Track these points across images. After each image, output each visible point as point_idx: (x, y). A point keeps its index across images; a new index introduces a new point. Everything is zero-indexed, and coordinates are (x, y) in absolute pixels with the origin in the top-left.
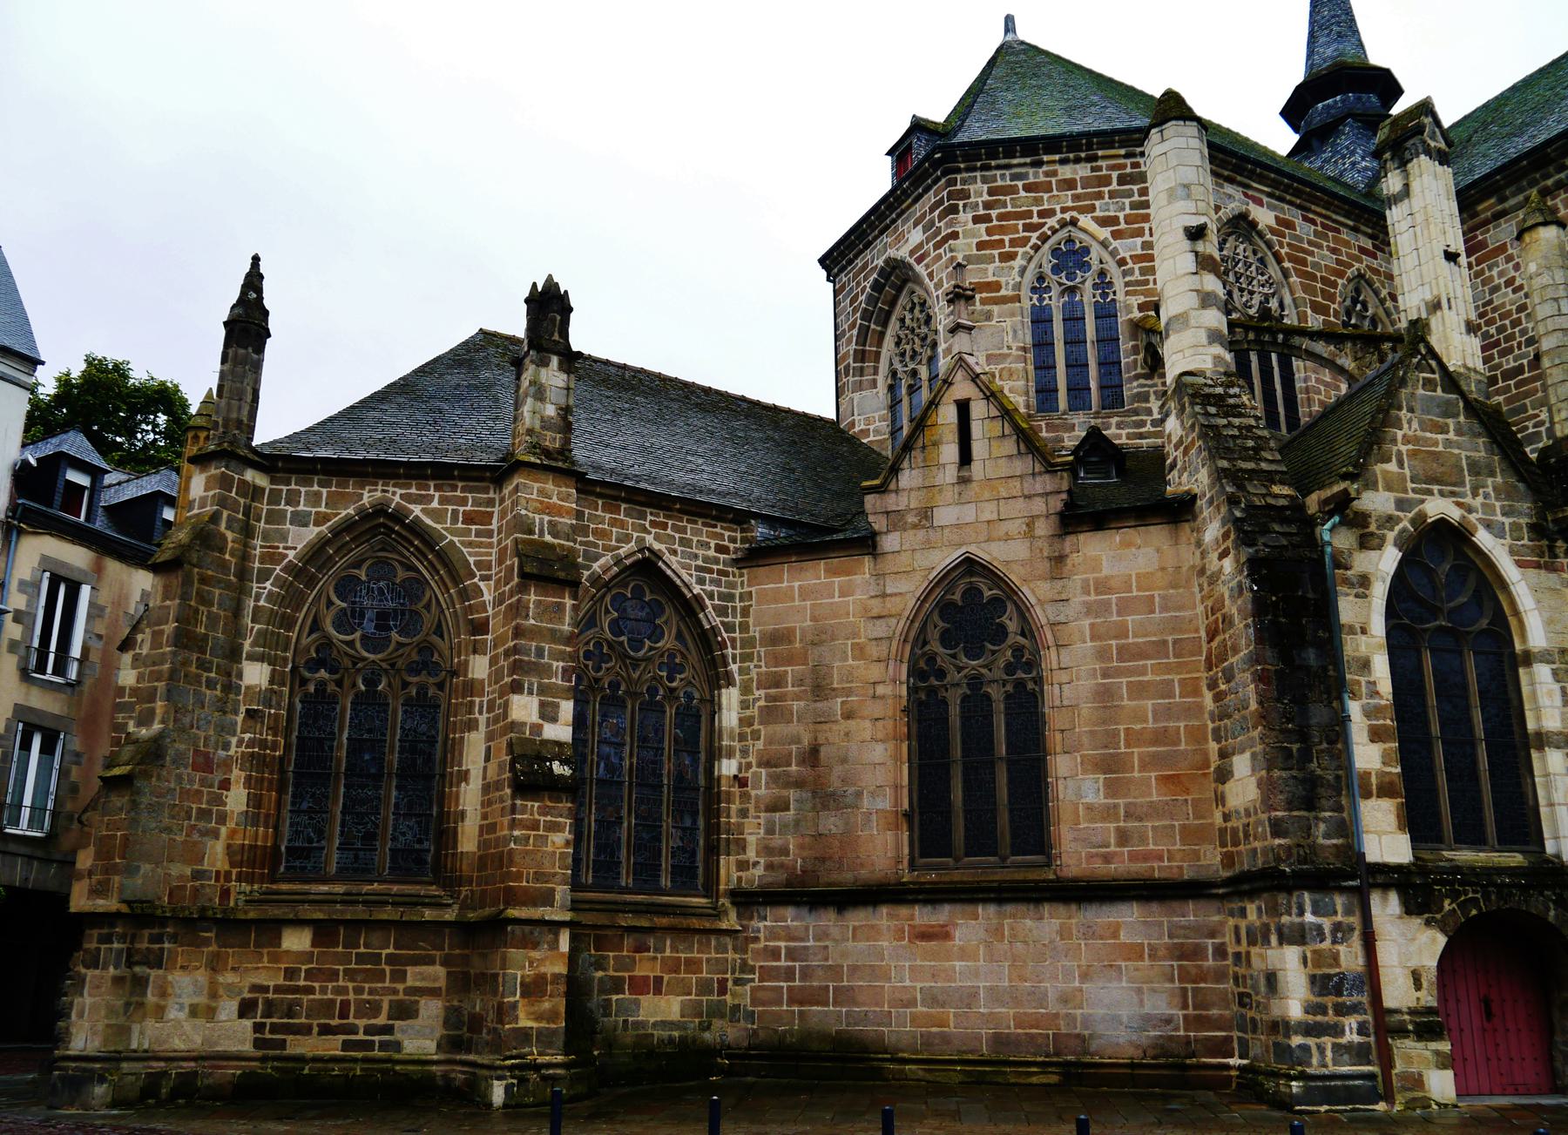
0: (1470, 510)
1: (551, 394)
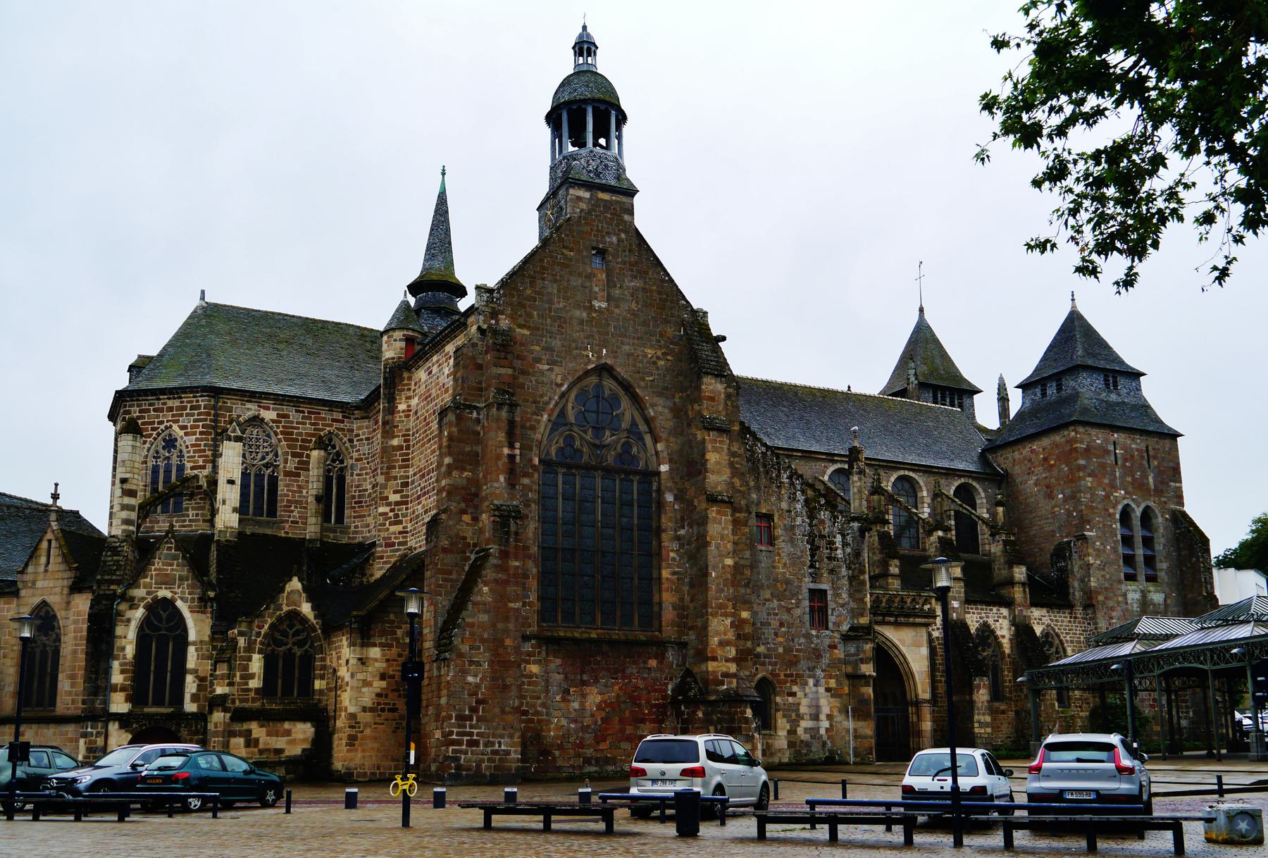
0: (175, 593)
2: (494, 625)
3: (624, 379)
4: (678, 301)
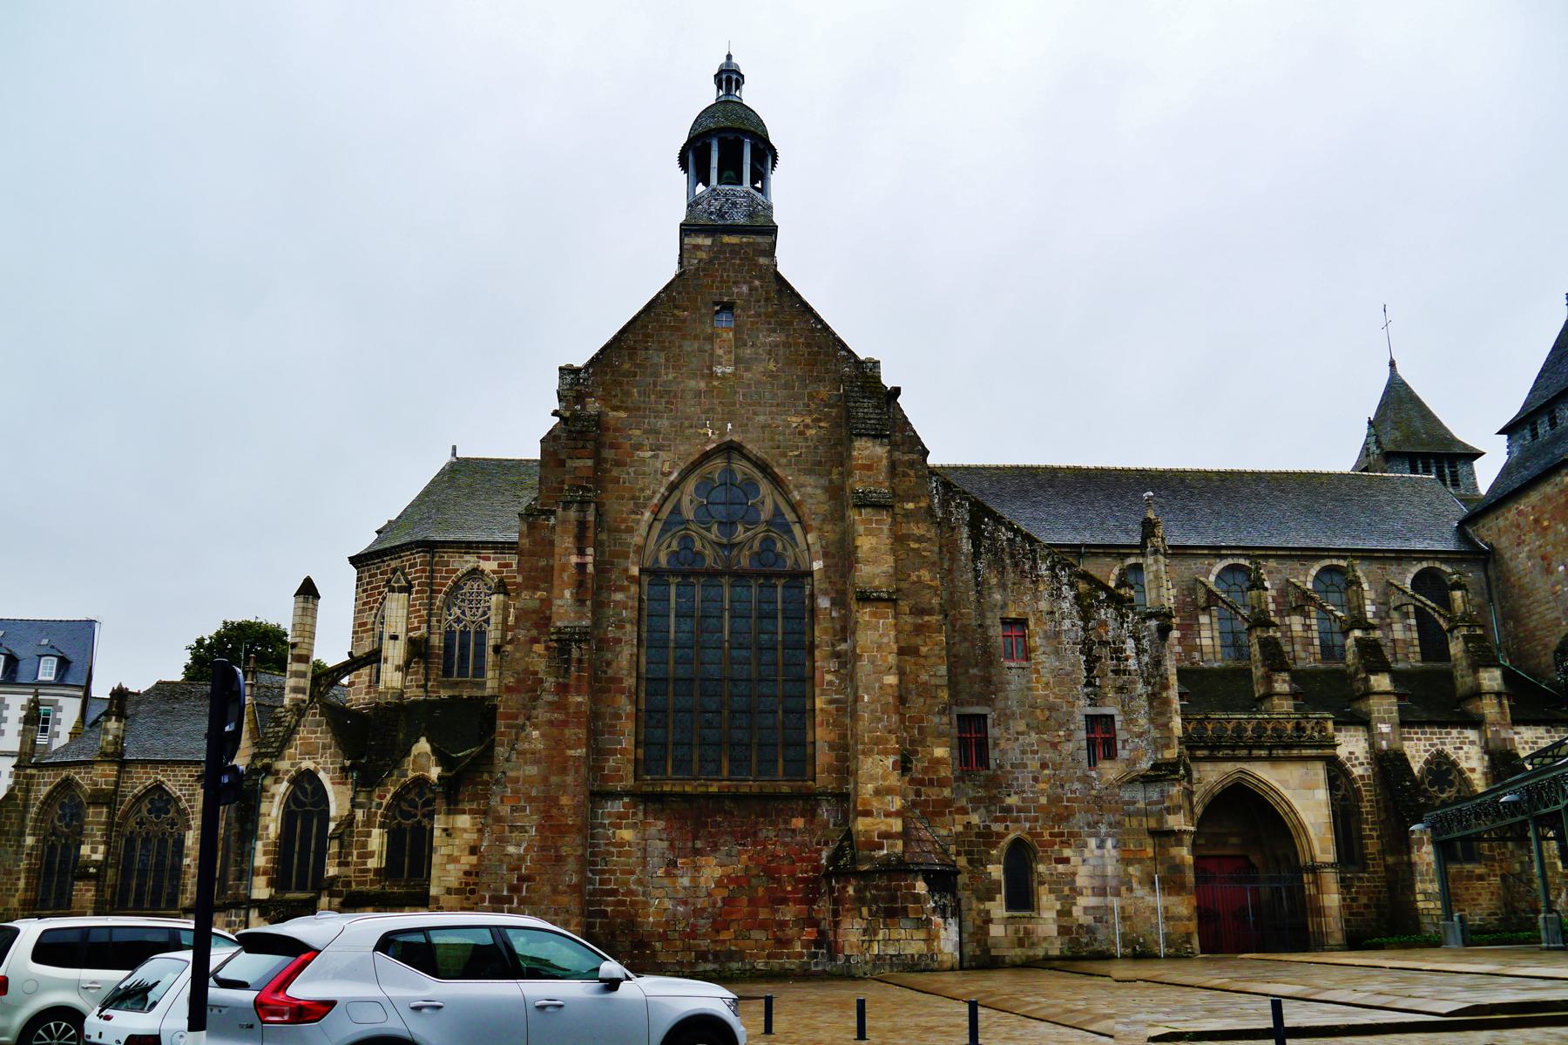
1: (111, 732)
2: (545, 779)
3: (758, 458)
4: (835, 353)
